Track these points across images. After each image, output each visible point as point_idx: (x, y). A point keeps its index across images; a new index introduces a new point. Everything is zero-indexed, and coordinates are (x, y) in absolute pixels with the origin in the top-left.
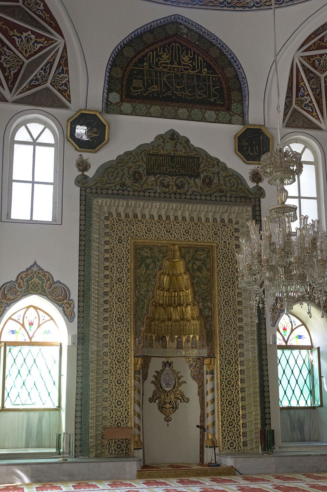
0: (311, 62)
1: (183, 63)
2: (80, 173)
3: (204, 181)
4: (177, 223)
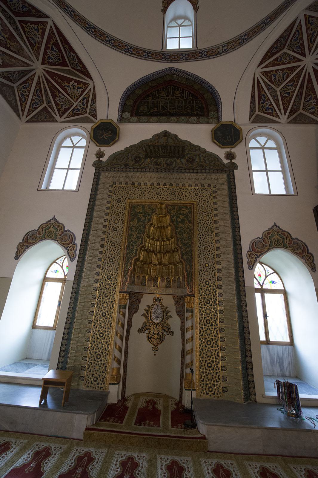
0: (269, 77)
1: (175, 95)
2: (98, 159)
3: (188, 160)
4: (165, 188)
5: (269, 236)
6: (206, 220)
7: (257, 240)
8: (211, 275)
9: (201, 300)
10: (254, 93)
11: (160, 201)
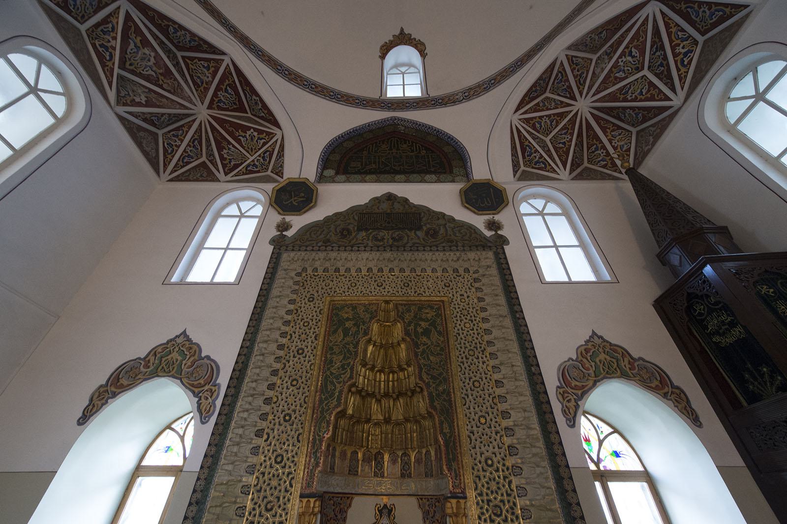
0: (531, 125)
2: (279, 233)
3: (427, 233)
4: (392, 275)
5: (589, 354)
6: (468, 329)
7: (568, 364)
8: (495, 443)
9: (481, 508)
10: (515, 143)
11: (383, 298)
